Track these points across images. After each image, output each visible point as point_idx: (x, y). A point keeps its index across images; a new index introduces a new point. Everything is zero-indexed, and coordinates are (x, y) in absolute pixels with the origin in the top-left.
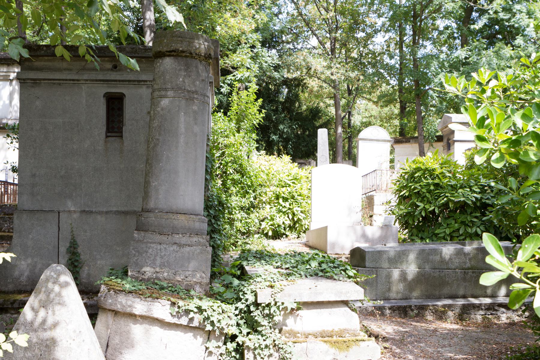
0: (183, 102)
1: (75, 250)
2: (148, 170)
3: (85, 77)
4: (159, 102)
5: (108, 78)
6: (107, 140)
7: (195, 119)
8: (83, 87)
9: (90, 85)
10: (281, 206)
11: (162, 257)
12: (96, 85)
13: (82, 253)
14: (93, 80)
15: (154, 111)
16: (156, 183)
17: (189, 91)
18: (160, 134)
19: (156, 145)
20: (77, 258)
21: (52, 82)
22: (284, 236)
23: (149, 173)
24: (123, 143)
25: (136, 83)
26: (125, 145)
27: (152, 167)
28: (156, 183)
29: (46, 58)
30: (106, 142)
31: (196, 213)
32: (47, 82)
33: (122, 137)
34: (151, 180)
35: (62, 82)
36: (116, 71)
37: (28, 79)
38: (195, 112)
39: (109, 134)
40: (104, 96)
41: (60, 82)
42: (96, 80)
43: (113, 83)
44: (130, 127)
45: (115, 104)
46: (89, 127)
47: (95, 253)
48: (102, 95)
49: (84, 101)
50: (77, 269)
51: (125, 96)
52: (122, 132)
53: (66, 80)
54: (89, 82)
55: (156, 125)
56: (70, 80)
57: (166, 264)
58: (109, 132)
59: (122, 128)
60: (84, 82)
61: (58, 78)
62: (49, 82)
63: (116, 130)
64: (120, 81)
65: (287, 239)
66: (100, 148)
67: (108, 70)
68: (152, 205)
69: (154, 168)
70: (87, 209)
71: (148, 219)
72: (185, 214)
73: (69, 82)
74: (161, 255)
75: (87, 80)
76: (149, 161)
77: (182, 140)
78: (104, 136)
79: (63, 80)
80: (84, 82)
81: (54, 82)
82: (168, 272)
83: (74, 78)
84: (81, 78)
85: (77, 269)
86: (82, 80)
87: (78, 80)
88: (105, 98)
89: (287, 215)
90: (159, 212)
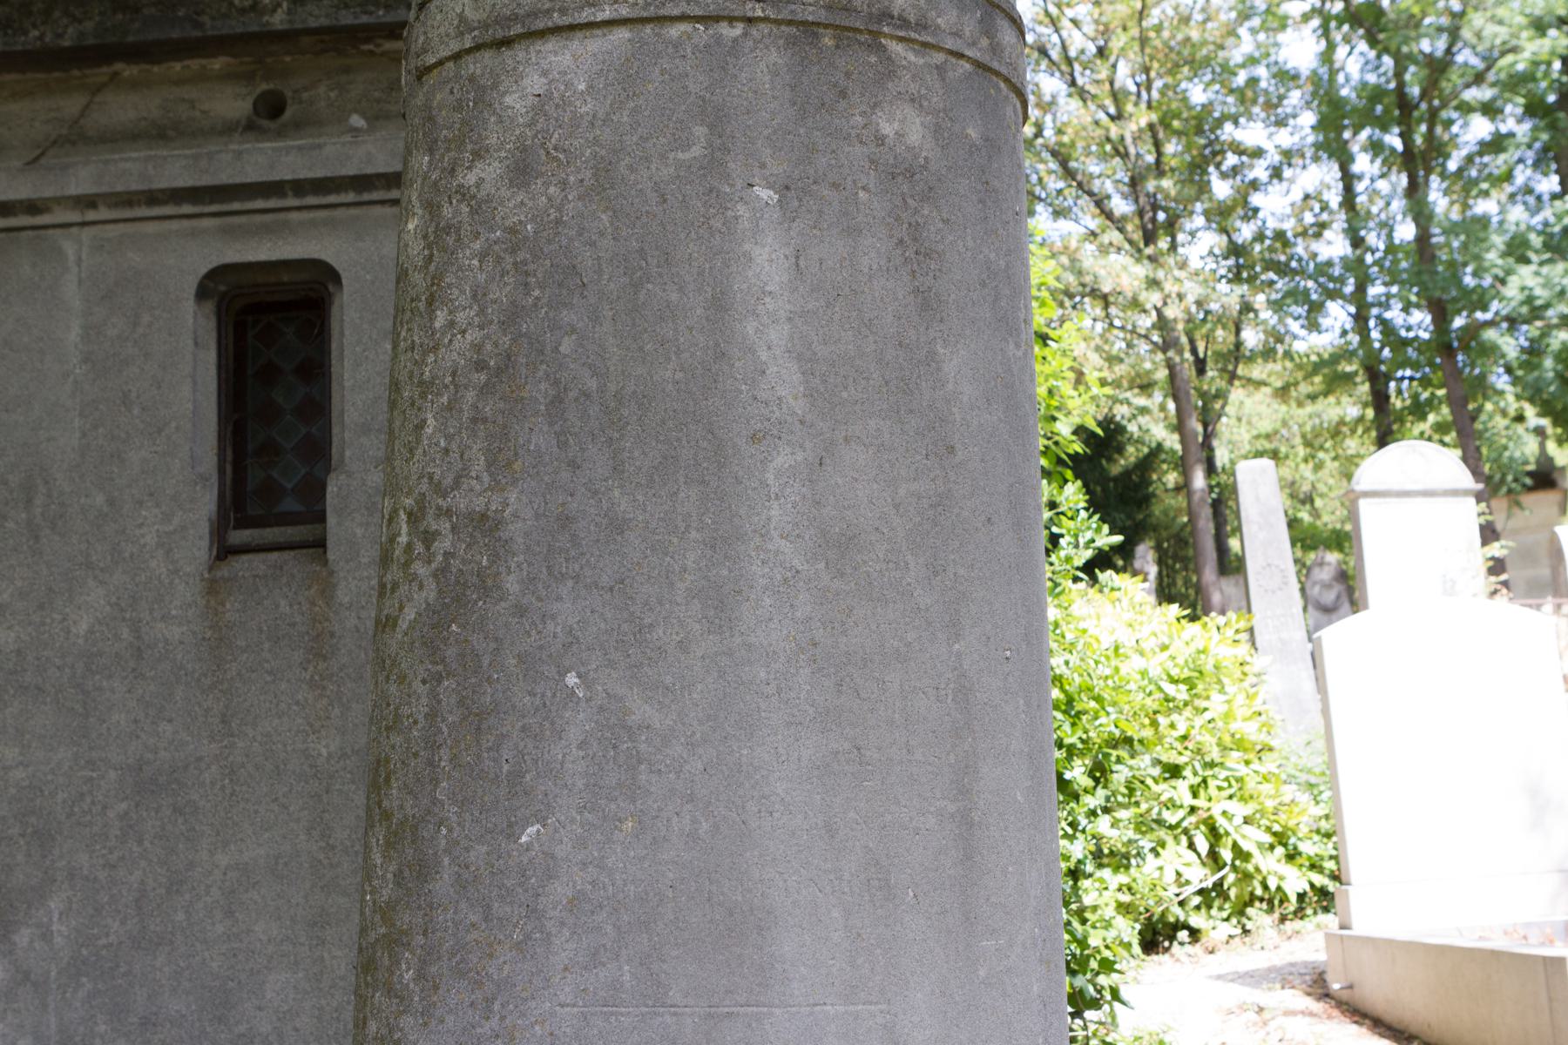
0: (764, 64)
2: (387, 912)
3: (81, 181)
4: (483, 95)
5: (224, 178)
6: (224, 571)
7: (916, 251)
8: (69, 249)
15: (432, 208)
18: (500, 465)
19: (461, 595)
22: (1183, 935)
23: (395, 941)
24: (327, 590)
27: (424, 870)
30: (212, 588)
33: (320, 544)
36: (280, 134)
38: (902, 173)
39: (238, 537)
40: (202, 293)
43: (259, 204)
45: (273, 338)
46: (100, 499)
49: (74, 334)
51: (332, 275)
52: (321, 518)
54: (103, 213)
55: (457, 351)
58: (242, 524)
59: (323, 487)
60: (74, 217)
63: (290, 505)
64: (300, 187)
65: (1197, 949)
66: (175, 632)
67: (228, 129)
69: (443, 884)
75: (89, 202)
76: (394, 797)
77: (777, 502)
78: (198, 547)
80: (74, 217)
84: (49, 192)
86: (60, 201)
87: (32, 207)
88: (210, 306)
89: (1184, 839)
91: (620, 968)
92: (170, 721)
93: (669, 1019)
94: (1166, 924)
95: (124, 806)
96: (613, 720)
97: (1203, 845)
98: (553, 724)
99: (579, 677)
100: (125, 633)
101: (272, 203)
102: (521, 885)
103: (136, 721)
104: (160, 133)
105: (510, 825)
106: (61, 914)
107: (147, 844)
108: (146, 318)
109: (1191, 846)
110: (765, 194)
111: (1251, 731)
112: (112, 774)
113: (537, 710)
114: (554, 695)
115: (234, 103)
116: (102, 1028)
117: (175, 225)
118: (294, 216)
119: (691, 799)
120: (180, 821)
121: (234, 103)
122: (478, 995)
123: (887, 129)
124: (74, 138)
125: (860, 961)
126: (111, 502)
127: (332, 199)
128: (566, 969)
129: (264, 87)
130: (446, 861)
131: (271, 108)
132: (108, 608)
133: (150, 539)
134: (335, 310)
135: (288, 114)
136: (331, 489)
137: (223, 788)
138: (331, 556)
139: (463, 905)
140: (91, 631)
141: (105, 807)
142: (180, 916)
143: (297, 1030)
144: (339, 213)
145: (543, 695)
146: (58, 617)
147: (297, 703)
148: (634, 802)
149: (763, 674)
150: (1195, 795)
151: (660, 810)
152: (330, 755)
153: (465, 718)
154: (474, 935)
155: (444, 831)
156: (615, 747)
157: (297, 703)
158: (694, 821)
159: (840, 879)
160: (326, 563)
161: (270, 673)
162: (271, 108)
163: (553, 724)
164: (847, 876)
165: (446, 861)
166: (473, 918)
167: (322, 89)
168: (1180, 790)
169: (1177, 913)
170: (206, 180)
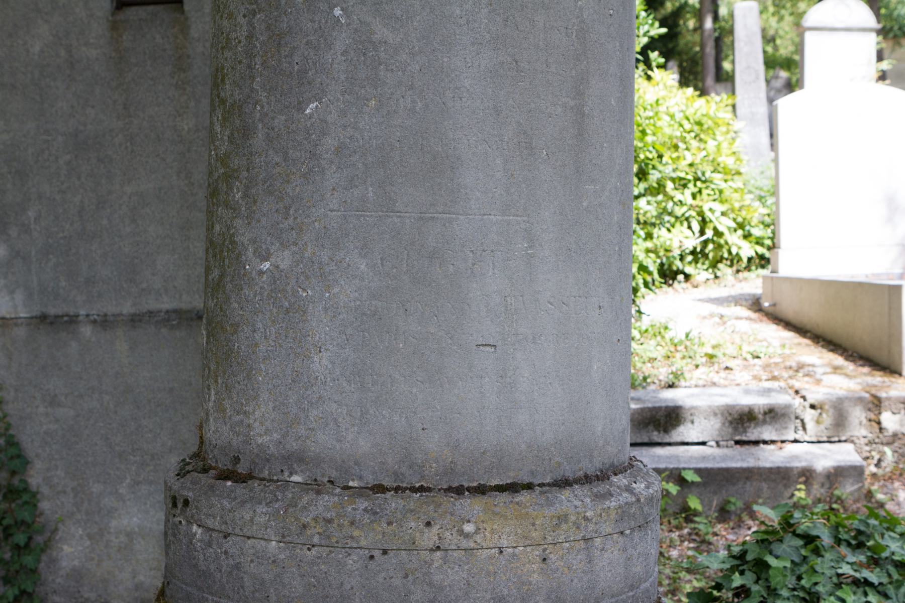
2: (224, 160)
6: (121, 16)
10: (672, 198)
16: (285, 259)
22: (681, 277)
23: (230, 176)
24: (185, 29)
27: (246, 132)
28: (285, 259)
30: (114, 26)
31: (591, 468)
34: (244, 237)
65: (688, 285)
68: (262, 426)
69: (258, 140)
72: (513, 488)
89: (685, 224)
90: (315, 487)
91: (367, 189)
92: (93, 107)
93: (396, 220)
94: (671, 271)
95: (68, 157)
96: (364, 37)
97: (696, 227)
98: (326, 39)
99: (342, 10)
100: (63, 53)
102: (306, 139)
103: (72, 107)
105: (299, 103)
106: (35, 219)
107: (83, 179)
109: (690, 227)
111: (728, 161)
112: (60, 138)
113: (316, 31)
114: (326, 22)
116: (63, 284)
119: (412, 87)
120: (102, 166)
122: (281, 205)
125: (513, 190)
128: (334, 189)
130: (260, 126)
132: (51, 38)
137: (126, 148)
138: (186, 7)
139: (271, 152)
140: (42, 51)
141: (57, 158)
142: (105, 222)
143: (175, 287)
145: (320, 22)
146: (21, 42)
147: (169, 98)
148: (376, 89)
149: (458, 12)
151: (392, 94)
152: (189, 130)
153: (271, 38)
154: (278, 170)
155: (259, 108)
156: (364, 54)
157: (169, 98)
158: (413, 101)
159: (502, 140)
160: (183, 12)
161: (152, 79)
163: (326, 39)
164: (506, 139)
165: (260, 126)
166: (277, 159)
168: (686, 196)
169: (678, 264)
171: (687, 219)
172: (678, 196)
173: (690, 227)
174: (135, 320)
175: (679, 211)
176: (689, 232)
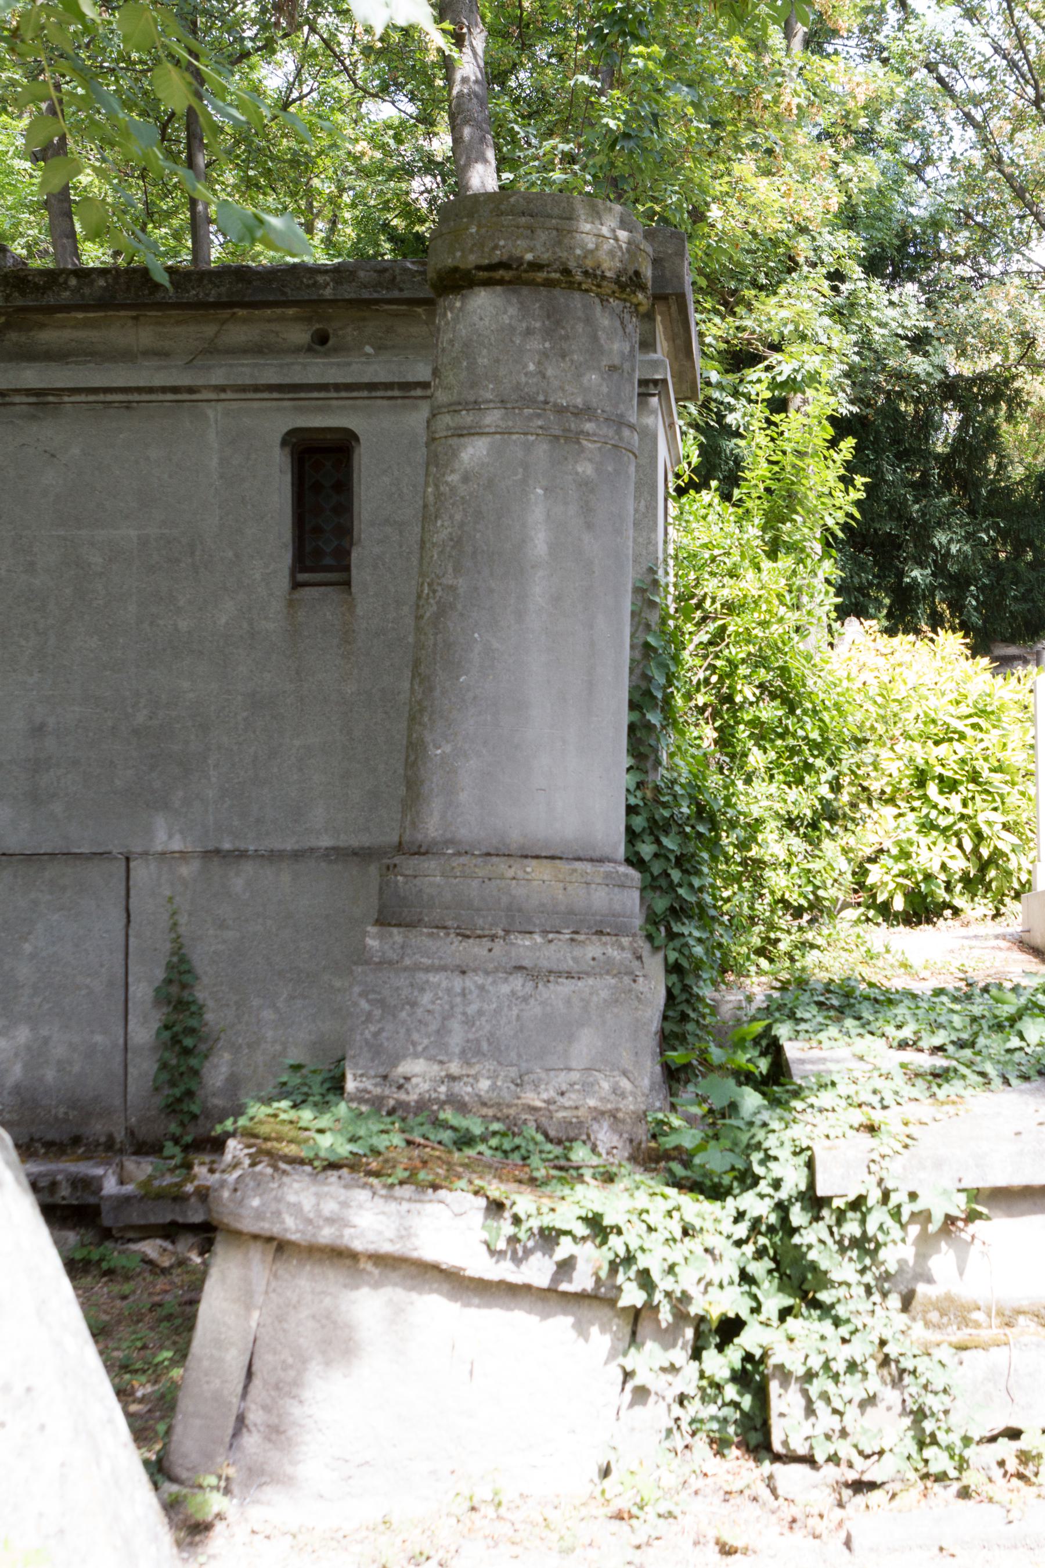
0: (542, 449)
1: (185, 994)
3: (218, 377)
4: (455, 453)
5: (297, 380)
7: (587, 509)
8: (211, 414)
9: (235, 405)
11: (469, 1022)
12: (256, 405)
13: (211, 1003)
14: (243, 389)
15: (437, 486)
16: (448, 748)
17: (560, 410)
20: (193, 1023)
21: (101, 397)
23: (422, 711)
24: (352, 608)
25: (396, 393)
26: (359, 611)
27: (431, 689)
28: (448, 748)
29: (80, 315)
30: (291, 604)
32: (82, 398)
33: (347, 583)
34: (428, 738)
35: (136, 397)
36: (326, 354)
37: (17, 391)
38: (585, 485)
39: (302, 577)
40: (284, 443)
41: (128, 400)
42: (256, 388)
43: (315, 395)
44: (377, 550)
45: (322, 469)
46: (230, 554)
47: (256, 1002)
48: (278, 440)
50: (193, 1062)
51: (356, 438)
52: (347, 569)
53: (151, 390)
54: (229, 395)
55: (444, 534)
56: (164, 390)
57: (485, 1046)
58: (304, 569)
59: (348, 553)
61: (120, 383)
62: (91, 398)
63: (328, 561)
64: (337, 387)
66: (271, 626)
67: (297, 350)
68: (432, 827)
69: (437, 693)
70: (227, 846)
71: (417, 881)
73: (161, 397)
74: (464, 1014)
75: (222, 389)
76: (422, 669)
77: (539, 589)
78: (283, 581)
79: (139, 390)
81: (110, 397)
82: (493, 1077)
83: (179, 383)
84: (200, 382)
85: (193, 1062)
86: (205, 387)
87: (191, 390)
88: (287, 450)
90: (458, 854)
94: (937, 904)
97: (968, 845)
100: (245, 625)
101: (322, 395)
104: (259, 350)
108: (253, 456)
109: (960, 846)
110: (540, 491)
111: (1016, 758)
115: (300, 335)
117: (269, 404)
118: (334, 403)
121: (300, 335)
123: (580, 470)
124: (212, 350)
126: (237, 556)
127: (355, 394)
129: (318, 326)
131: (322, 339)
133: (258, 576)
134: (356, 457)
135: (331, 343)
136: (354, 555)
138: (354, 589)
144: (359, 402)
150: (965, 805)
162: (322, 339)
167: (349, 330)
168: (954, 802)
169: (942, 895)
170: (287, 381)
171: (956, 834)
172: (942, 801)
173: (960, 846)
174: (297, 855)
175: (943, 822)
176: (957, 852)
